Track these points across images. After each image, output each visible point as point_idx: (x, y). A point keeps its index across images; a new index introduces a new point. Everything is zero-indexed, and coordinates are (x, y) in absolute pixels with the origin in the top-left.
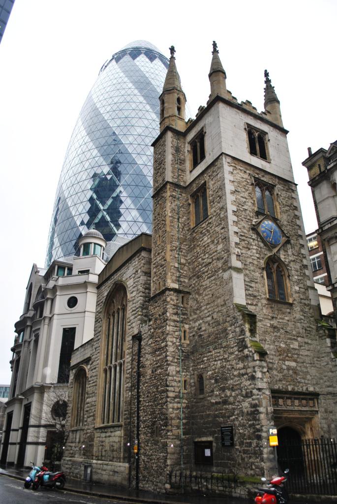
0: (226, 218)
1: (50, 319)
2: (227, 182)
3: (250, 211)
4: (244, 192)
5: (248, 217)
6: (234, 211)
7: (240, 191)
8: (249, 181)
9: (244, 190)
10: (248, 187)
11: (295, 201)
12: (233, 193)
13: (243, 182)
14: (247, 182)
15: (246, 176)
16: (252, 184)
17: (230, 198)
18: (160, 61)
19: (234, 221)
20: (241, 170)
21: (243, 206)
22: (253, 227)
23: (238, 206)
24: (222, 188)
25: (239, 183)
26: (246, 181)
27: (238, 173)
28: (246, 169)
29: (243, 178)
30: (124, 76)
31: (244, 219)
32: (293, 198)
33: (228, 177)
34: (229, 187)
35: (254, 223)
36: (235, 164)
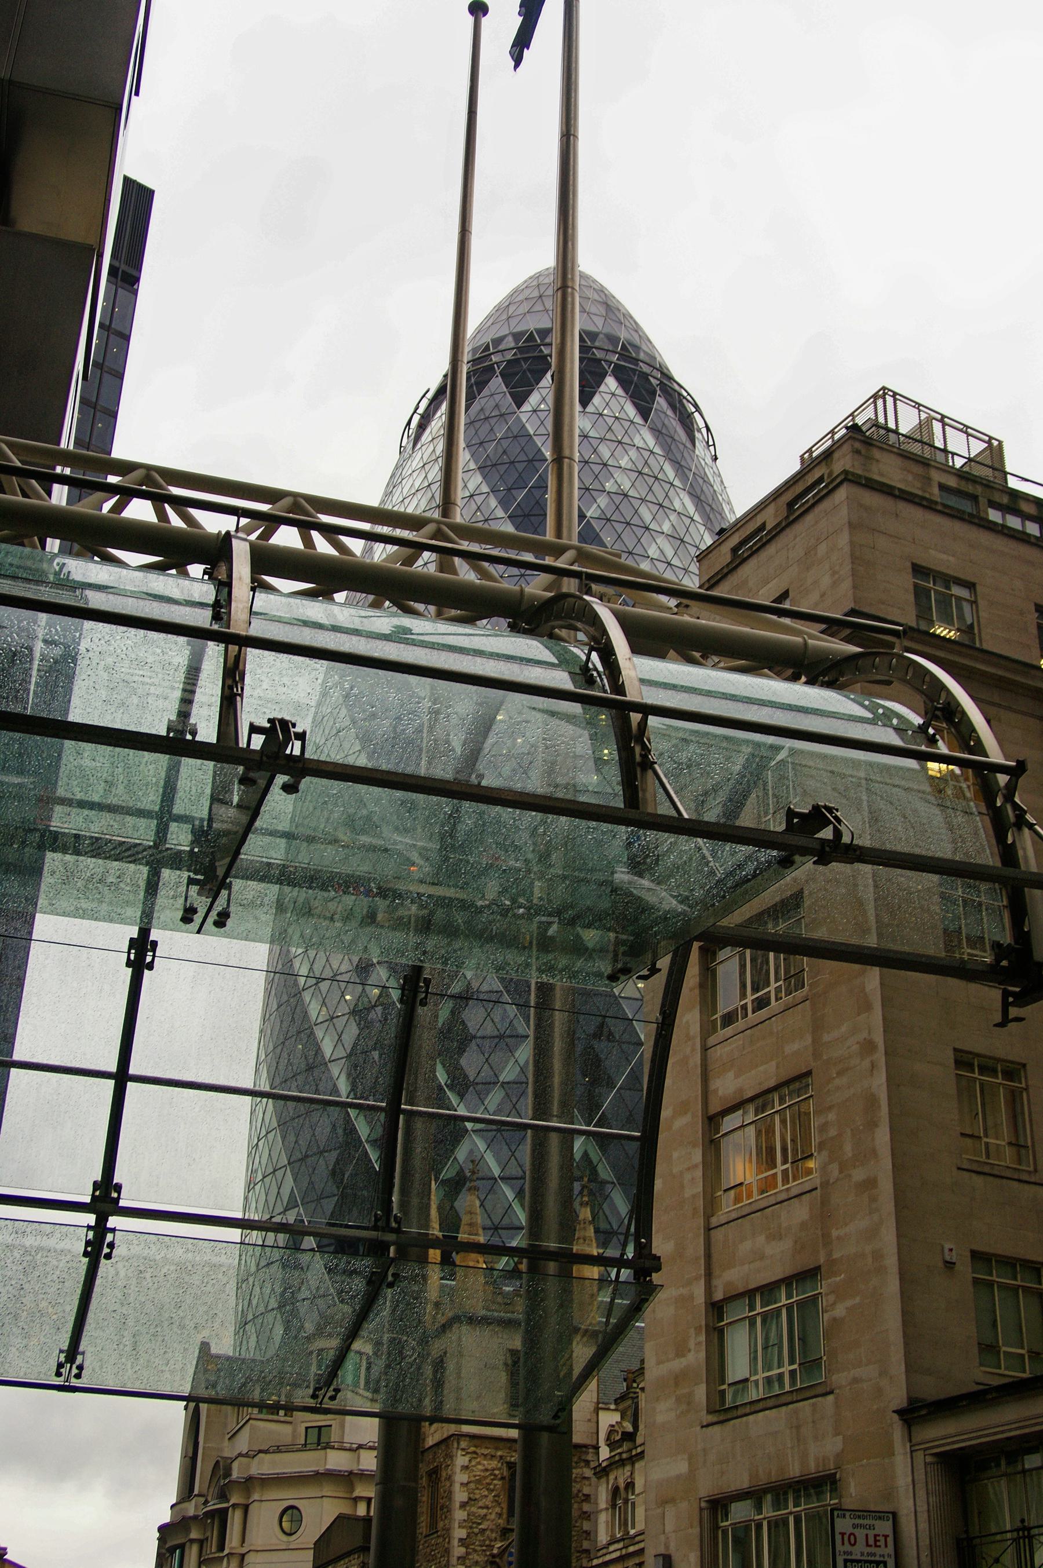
0: (447, 1551)
1: (243, 1556)
2: (457, 1487)
3: (492, 1531)
4: (486, 1496)
5: (487, 1542)
6: (461, 1540)
7: (477, 1496)
8: (497, 1472)
9: (486, 1493)
10: (495, 1485)
11: (587, 1483)
12: (463, 1505)
13: (485, 1478)
14: (495, 1475)
15: (494, 1464)
16: (503, 1478)
17: (460, 1515)
18: (620, 392)
19: (459, 1558)
20: (485, 1456)
21: (480, 1524)
22: (491, 1559)
23: (471, 1528)
24: (450, 1494)
25: (478, 1482)
26: (491, 1475)
27: (479, 1463)
28: (497, 1449)
29: (487, 1470)
30: (485, 489)
31: (479, 1548)
32: (585, 1478)
33: (461, 1477)
34: (460, 1495)
35: (495, 1551)
36: (476, 1446)
